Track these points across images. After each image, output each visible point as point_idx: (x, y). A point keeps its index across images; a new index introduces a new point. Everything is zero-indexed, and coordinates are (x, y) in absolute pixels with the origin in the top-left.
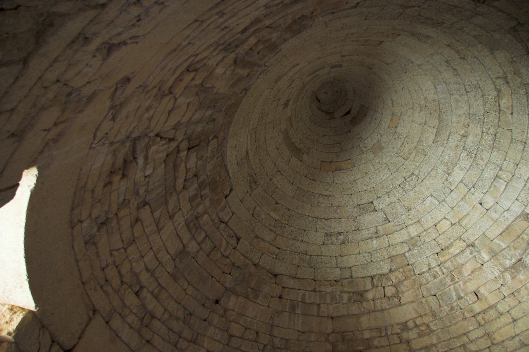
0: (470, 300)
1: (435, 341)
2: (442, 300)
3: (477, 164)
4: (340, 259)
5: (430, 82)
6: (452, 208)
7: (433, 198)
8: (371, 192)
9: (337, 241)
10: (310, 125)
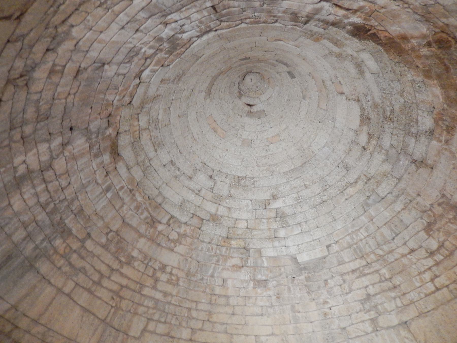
0: (218, 282)
1: (174, 293)
2: (201, 269)
3: (295, 208)
5: (325, 141)
6: (256, 218)
7: (250, 202)
8: (219, 163)
9: (173, 172)
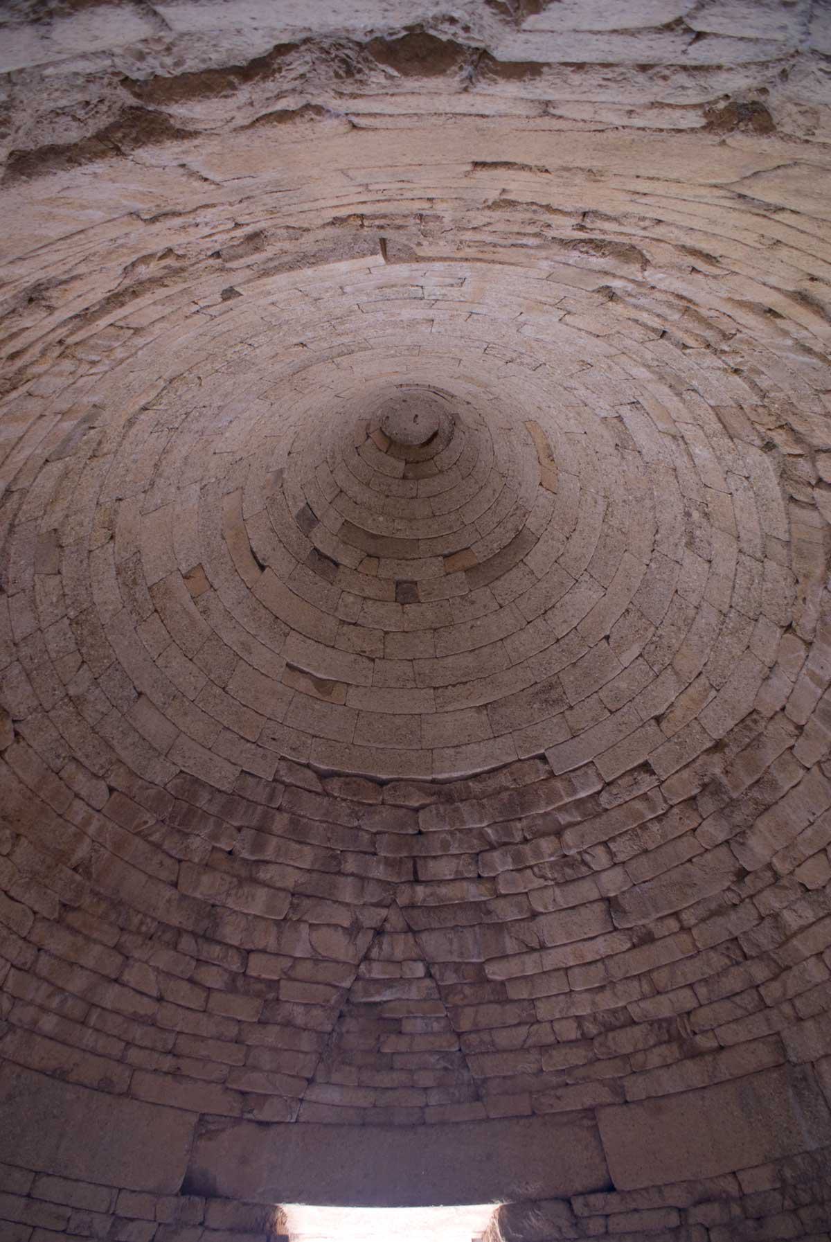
4: (744, 545)
8: (579, 414)
10: (476, 482)
